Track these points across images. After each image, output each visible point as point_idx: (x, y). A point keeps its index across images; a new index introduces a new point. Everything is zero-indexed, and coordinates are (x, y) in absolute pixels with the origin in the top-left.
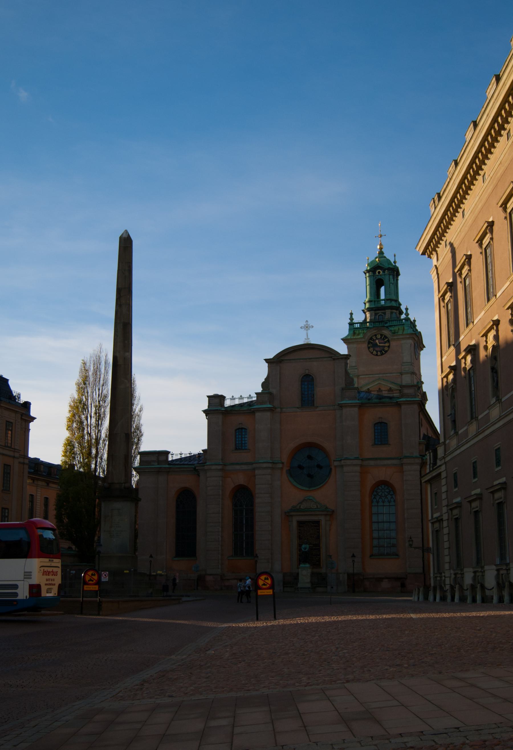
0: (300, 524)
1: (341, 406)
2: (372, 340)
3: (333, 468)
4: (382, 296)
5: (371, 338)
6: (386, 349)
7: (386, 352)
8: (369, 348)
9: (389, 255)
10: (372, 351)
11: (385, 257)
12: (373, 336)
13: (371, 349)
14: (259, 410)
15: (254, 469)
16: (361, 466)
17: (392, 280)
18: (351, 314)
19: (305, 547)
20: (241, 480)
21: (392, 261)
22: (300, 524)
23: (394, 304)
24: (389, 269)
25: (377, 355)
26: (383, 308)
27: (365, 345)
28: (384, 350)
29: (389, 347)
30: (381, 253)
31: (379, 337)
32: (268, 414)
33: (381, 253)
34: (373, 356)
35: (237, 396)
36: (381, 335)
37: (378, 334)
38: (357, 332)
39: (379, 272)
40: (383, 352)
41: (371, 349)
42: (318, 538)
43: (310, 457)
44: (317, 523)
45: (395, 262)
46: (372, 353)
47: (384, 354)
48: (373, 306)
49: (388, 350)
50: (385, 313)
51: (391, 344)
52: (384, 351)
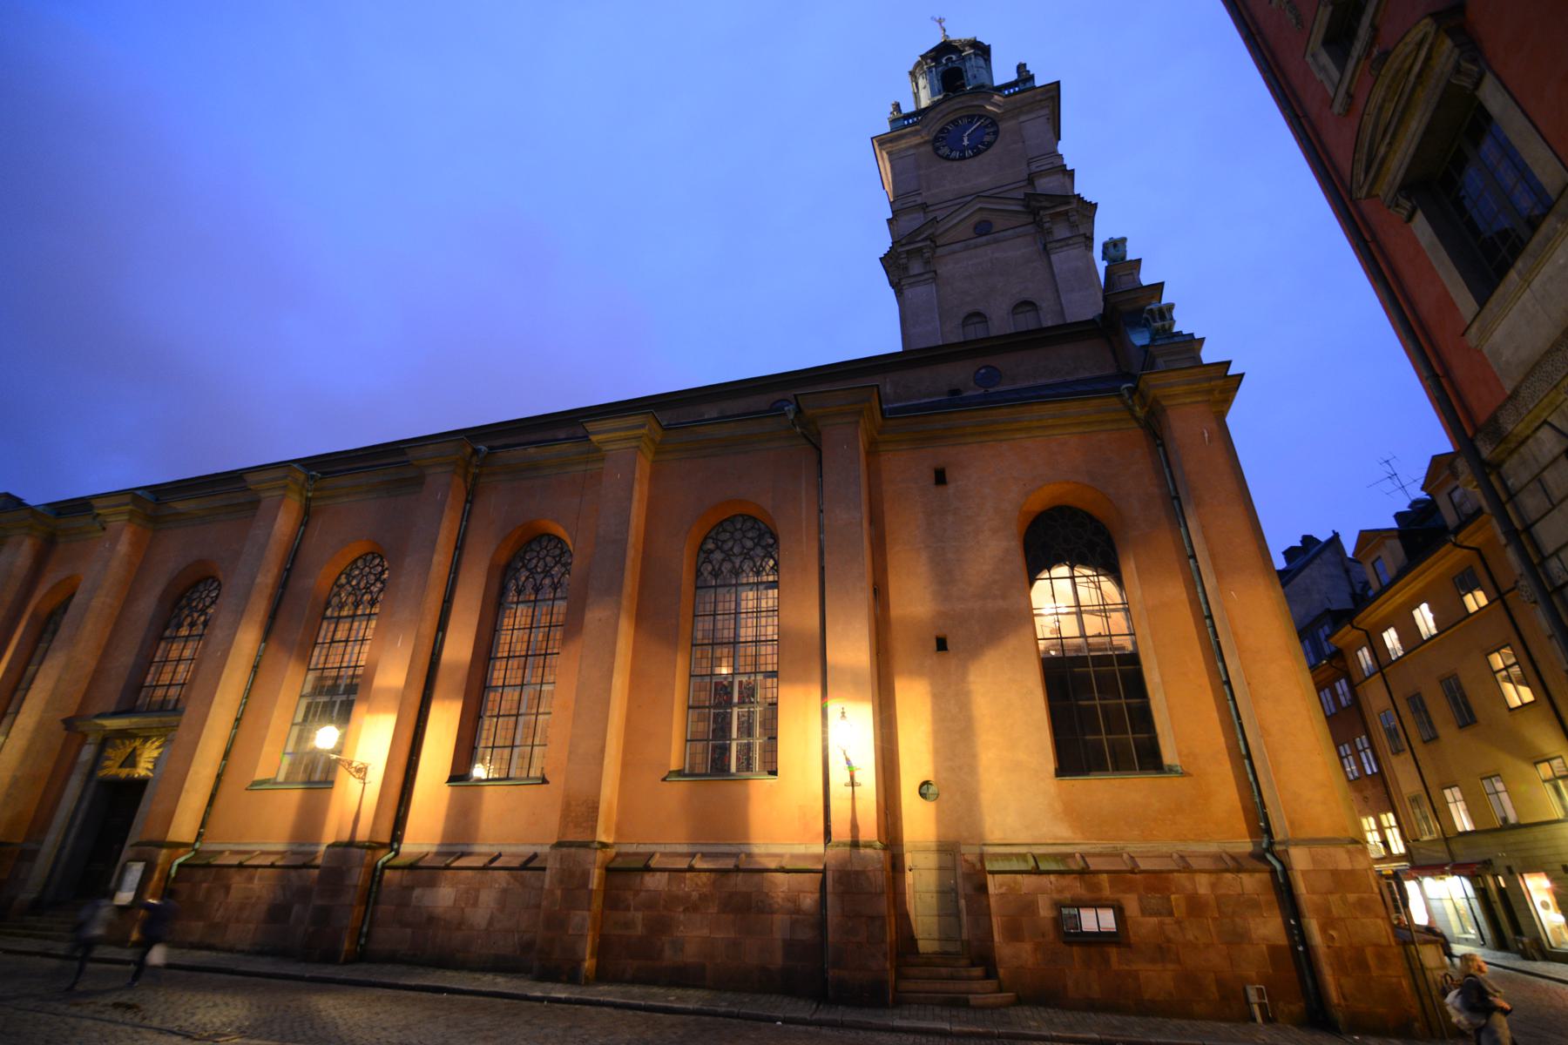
2: (944, 133)
6: (987, 139)
7: (989, 145)
10: (948, 152)
12: (947, 124)
13: (945, 151)
25: (963, 158)
27: (929, 148)
28: (982, 143)
29: (996, 133)
34: (948, 164)
37: (960, 118)
46: (947, 158)
47: (986, 150)
49: (994, 142)
51: (1000, 127)
52: (984, 145)
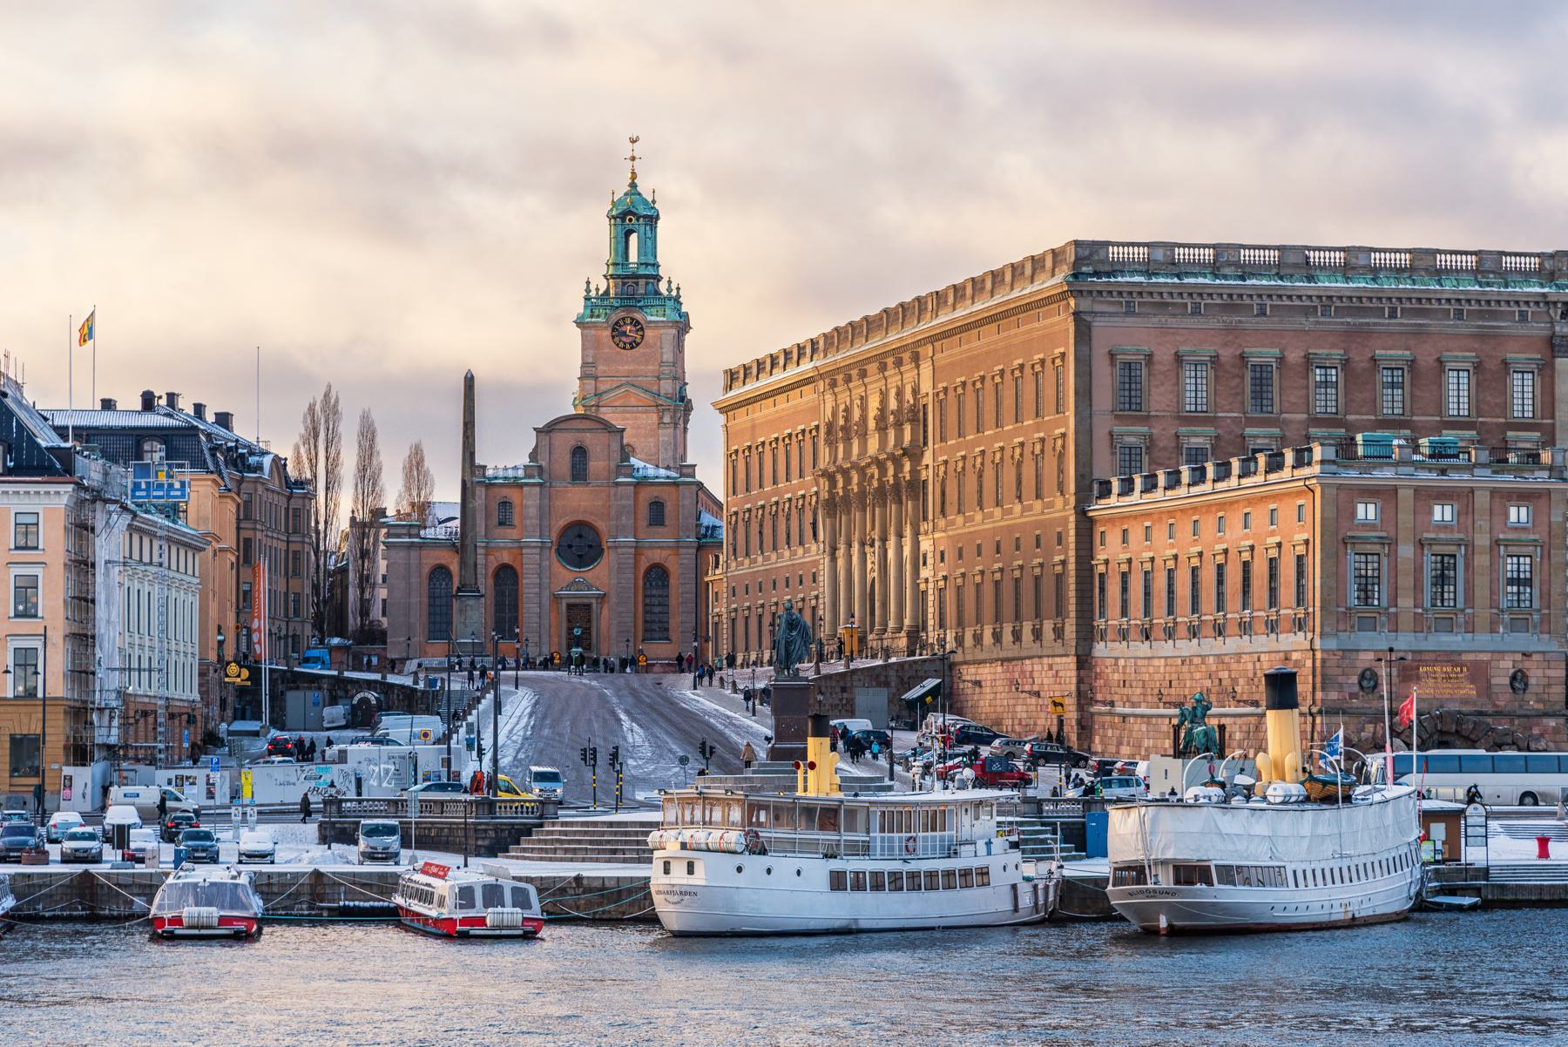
0: (569, 606)
1: (618, 484)
3: (605, 547)
4: (633, 256)
5: (617, 323)
7: (638, 344)
8: (613, 337)
9: (644, 188)
11: (639, 194)
14: (527, 484)
15: (521, 548)
16: (636, 548)
17: (649, 234)
18: (588, 283)
19: (577, 632)
20: (506, 558)
21: (650, 200)
22: (569, 606)
23: (650, 271)
24: (645, 217)
26: (636, 276)
30: (633, 185)
31: (629, 321)
32: (538, 489)
33: (633, 185)
35: (501, 466)
36: (632, 319)
38: (596, 312)
39: (630, 220)
40: (634, 345)
41: (617, 339)
42: (589, 621)
43: (580, 536)
44: (588, 607)
45: (654, 202)
48: (620, 272)
50: (637, 284)
